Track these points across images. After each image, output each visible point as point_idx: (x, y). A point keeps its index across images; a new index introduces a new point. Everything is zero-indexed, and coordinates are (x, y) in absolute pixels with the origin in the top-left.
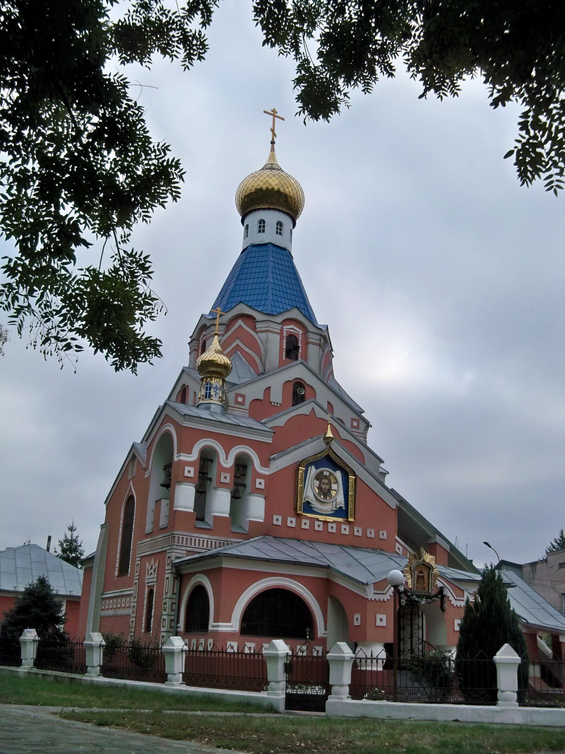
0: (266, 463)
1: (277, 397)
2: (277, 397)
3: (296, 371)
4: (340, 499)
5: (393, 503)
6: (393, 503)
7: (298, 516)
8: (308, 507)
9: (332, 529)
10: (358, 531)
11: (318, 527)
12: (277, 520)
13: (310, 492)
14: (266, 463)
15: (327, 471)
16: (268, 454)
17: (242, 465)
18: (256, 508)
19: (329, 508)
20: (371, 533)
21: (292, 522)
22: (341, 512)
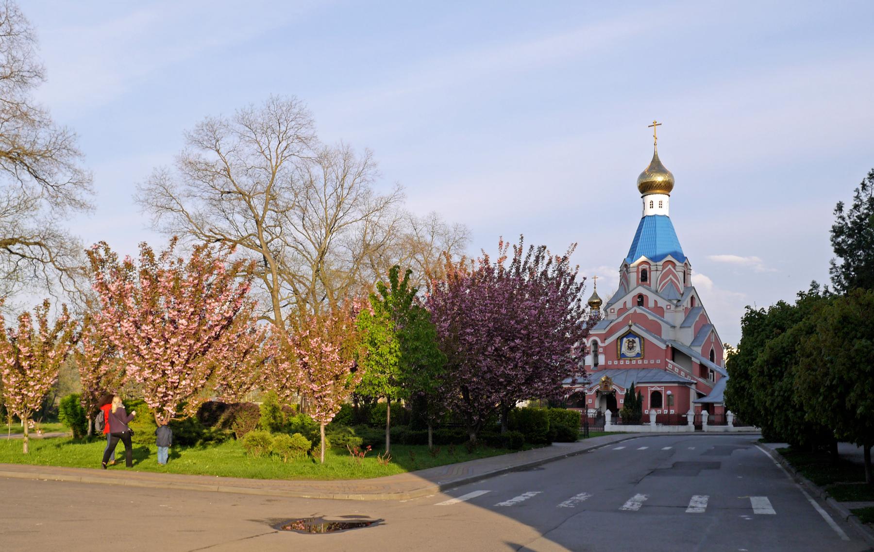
0: (603, 342)
1: (629, 305)
2: (629, 305)
3: (641, 290)
4: (638, 349)
5: (663, 347)
6: (663, 347)
7: (619, 360)
8: (623, 356)
9: (634, 362)
10: (646, 362)
11: (628, 362)
12: (610, 363)
13: (624, 349)
14: (603, 342)
15: (631, 339)
16: (604, 338)
17: (595, 343)
18: (602, 360)
19: (632, 354)
20: (652, 362)
21: (616, 363)
22: (638, 355)
